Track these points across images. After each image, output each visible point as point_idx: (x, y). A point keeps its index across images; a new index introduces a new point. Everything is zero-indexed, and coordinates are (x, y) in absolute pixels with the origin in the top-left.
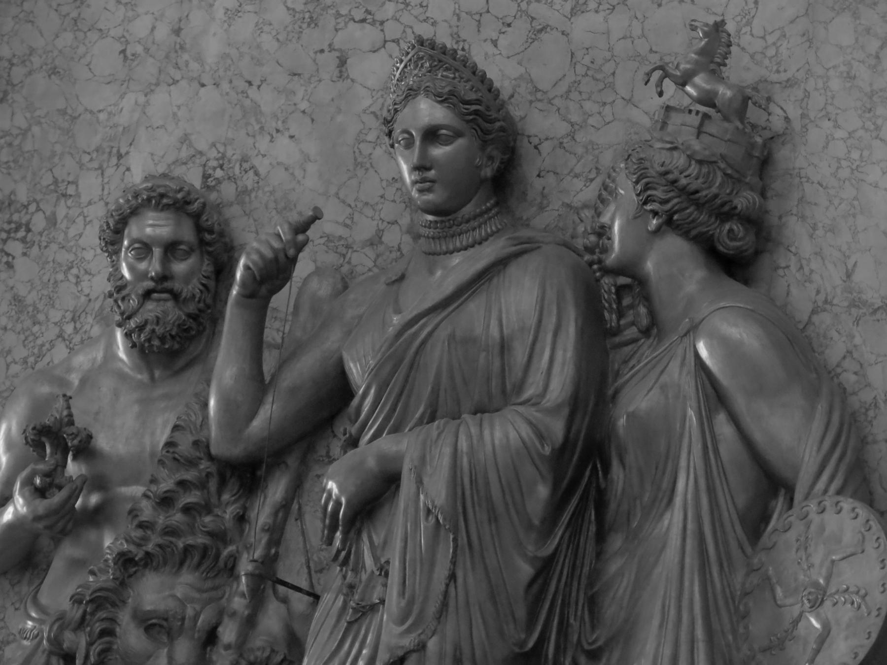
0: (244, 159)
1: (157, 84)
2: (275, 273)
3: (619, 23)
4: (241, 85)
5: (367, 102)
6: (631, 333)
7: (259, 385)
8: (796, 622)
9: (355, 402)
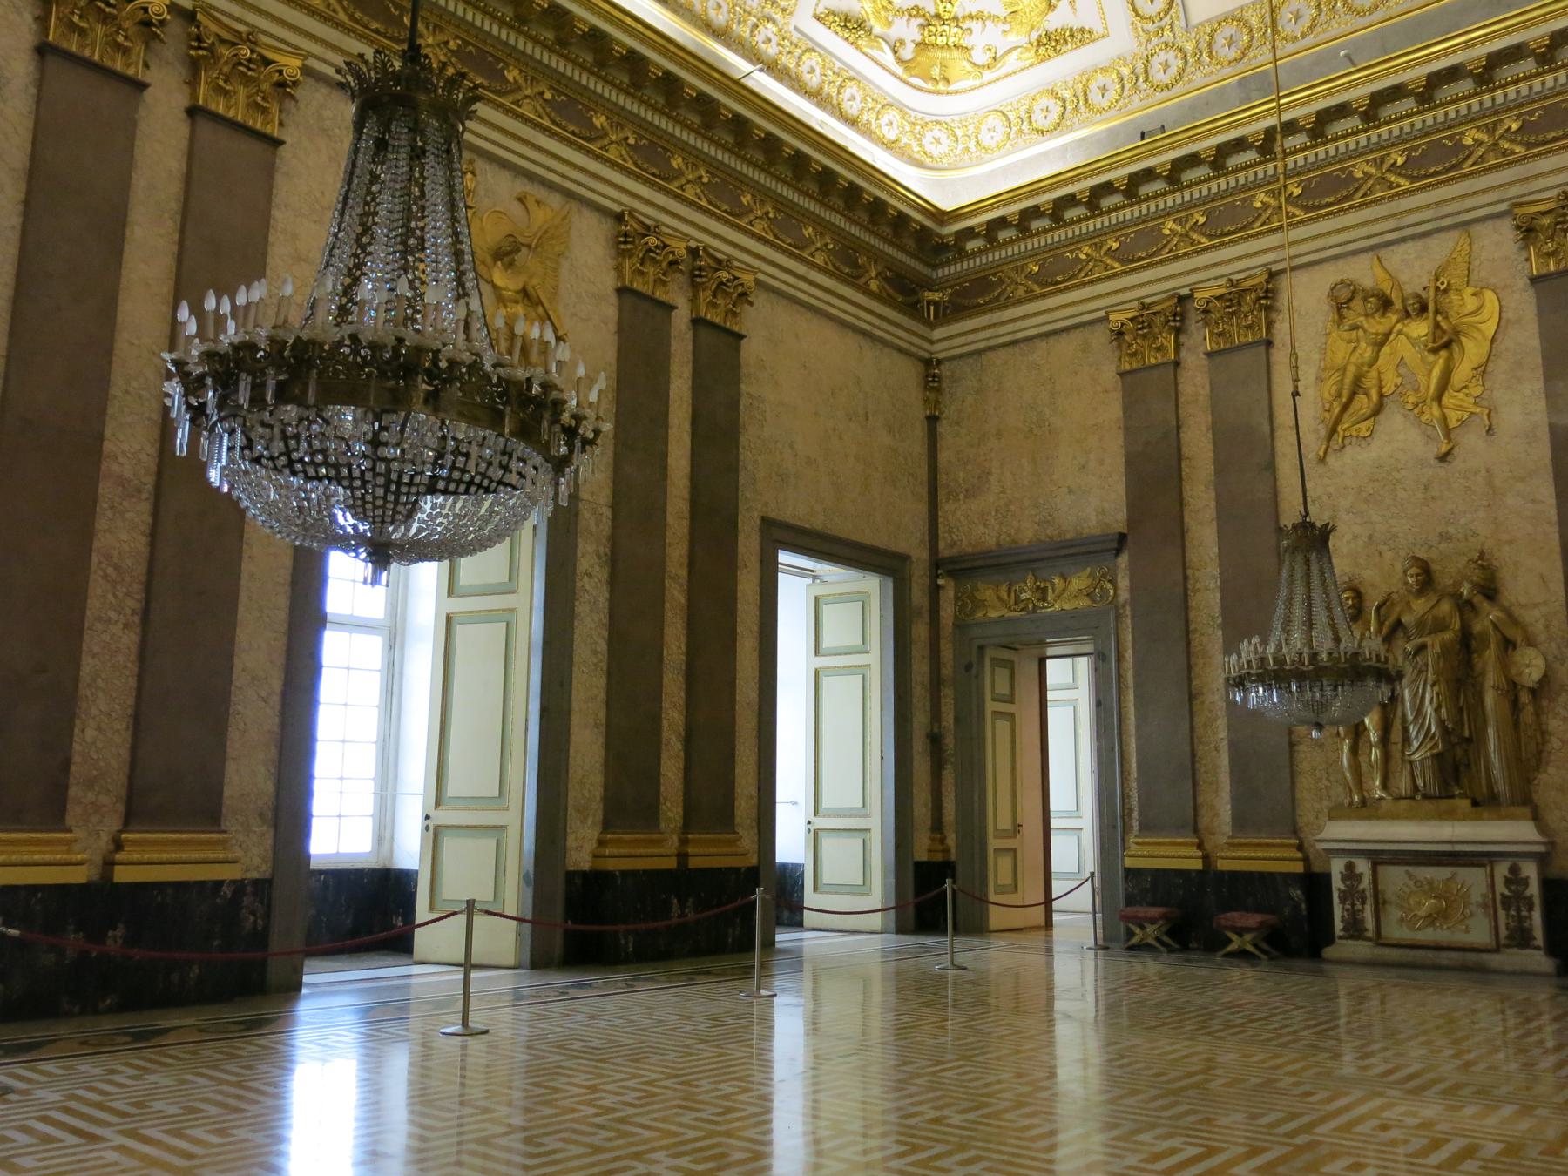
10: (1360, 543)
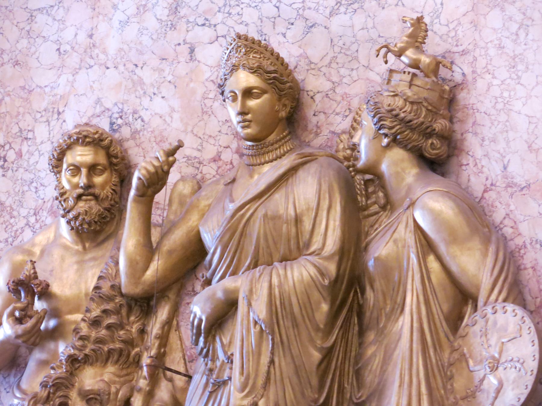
0: (135, 112)
1: (80, 69)
2: (156, 180)
3: (359, 20)
4: (131, 67)
5: (207, 75)
6: (375, 208)
7: (149, 250)
8: (482, 381)
9: (208, 258)
10: (151, 22)
